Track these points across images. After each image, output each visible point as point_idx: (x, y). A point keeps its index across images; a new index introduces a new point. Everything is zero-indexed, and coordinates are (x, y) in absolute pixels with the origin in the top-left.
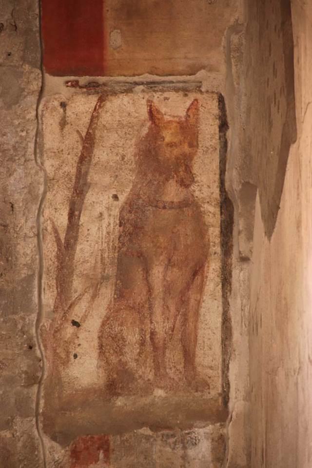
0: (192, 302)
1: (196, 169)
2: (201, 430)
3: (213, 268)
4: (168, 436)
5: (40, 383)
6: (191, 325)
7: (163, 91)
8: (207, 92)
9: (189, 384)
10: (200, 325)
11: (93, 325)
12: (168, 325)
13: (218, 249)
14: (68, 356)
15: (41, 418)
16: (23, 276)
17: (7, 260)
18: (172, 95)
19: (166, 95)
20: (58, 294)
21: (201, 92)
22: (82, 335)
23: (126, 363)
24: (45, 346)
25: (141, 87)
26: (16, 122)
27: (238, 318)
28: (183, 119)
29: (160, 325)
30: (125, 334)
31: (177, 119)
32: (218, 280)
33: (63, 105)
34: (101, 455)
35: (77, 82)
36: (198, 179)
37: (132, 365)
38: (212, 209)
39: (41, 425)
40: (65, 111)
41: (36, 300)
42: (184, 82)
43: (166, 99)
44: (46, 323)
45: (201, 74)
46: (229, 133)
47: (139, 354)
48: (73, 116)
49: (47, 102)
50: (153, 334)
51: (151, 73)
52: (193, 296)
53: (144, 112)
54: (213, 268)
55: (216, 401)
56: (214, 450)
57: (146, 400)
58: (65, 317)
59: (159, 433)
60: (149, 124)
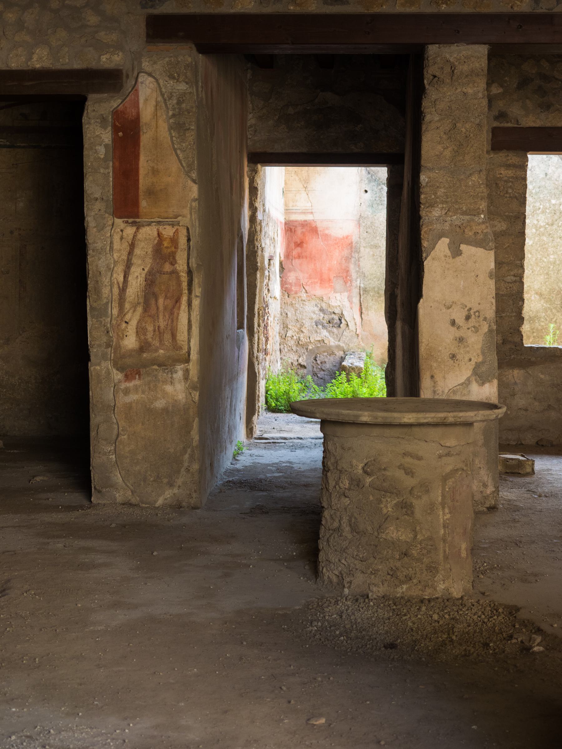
0: (175, 314)
1: (177, 258)
2: (179, 367)
3: (184, 299)
4: (165, 369)
5: (112, 347)
6: (175, 323)
7: (163, 225)
8: (182, 226)
9: (174, 348)
10: (179, 323)
11: (134, 323)
12: (165, 323)
13: (186, 291)
14: (123, 336)
15: (112, 361)
16: (104, 302)
17: (98, 296)
18: (167, 227)
19: (165, 227)
20: (119, 310)
21: (180, 226)
22: (129, 327)
23: (147, 339)
24: (114, 332)
25: (155, 223)
26: (102, 238)
27: (195, 321)
28: (172, 237)
29: (162, 323)
30: (147, 327)
31: (169, 237)
32: (186, 304)
33: (122, 231)
34: (137, 377)
35: (128, 221)
36: (178, 262)
37: (150, 340)
38: (184, 275)
39: (112, 364)
40: (122, 233)
41: (110, 313)
42: (173, 221)
43: (165, 228)
44: (114, 322)
45: (179, 218)
46: (191, 243)
47: (153, 335)
48: (126, 235)
49: (115, 229)
50: (159, 327)
51: (159, 218)
52: (176, 311)
53: (156, 233)
54: (184, 299)
55: (185, 355)
56: (184, 375)
57: (157, 354)
58: (122, 320)
59: (161, 368)
60: (158, 239)
